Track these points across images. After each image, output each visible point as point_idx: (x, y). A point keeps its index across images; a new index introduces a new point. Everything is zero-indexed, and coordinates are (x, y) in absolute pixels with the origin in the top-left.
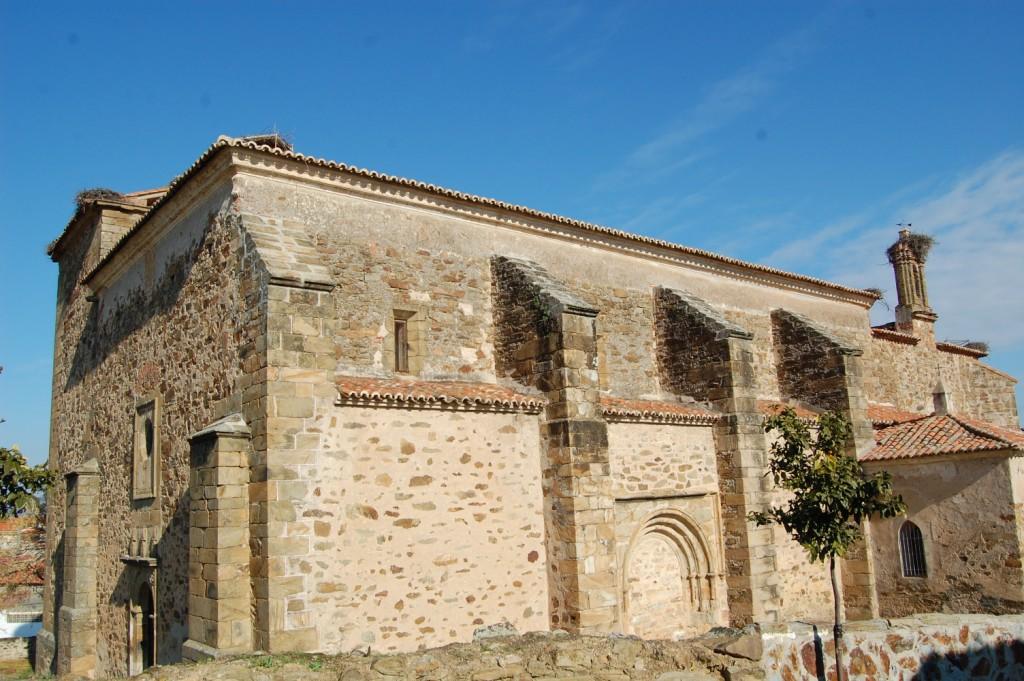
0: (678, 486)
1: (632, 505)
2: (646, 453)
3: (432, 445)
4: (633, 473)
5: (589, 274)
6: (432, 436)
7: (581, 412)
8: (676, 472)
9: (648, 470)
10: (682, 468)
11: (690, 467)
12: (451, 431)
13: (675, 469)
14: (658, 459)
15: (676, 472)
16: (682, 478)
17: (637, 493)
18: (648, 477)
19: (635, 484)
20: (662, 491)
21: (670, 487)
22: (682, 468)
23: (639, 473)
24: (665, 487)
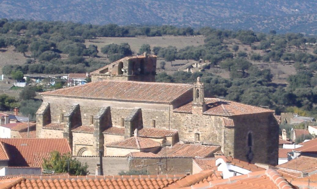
0: (88, 144)
1: (79, 145)
2: (82, 138)
3: (53, 134)
4: (79, 141)
5: (91, 105)
6: (53, 133)
7: (66, 131)
8: (88, 141)
9: (82, 140)
10: (89, 141)
11: (90, 140)
12: (55, 133)
13: (87, 140)
14: (84, 139)
15: (88, 141)
16: (88, 142)
17: (80, 144)
18: (82, 141)
19: (79, 142)
20: (84, 144)
21: (86, 143)
22: (89, 141)
23: (81, 141)
24: (85, 143)
